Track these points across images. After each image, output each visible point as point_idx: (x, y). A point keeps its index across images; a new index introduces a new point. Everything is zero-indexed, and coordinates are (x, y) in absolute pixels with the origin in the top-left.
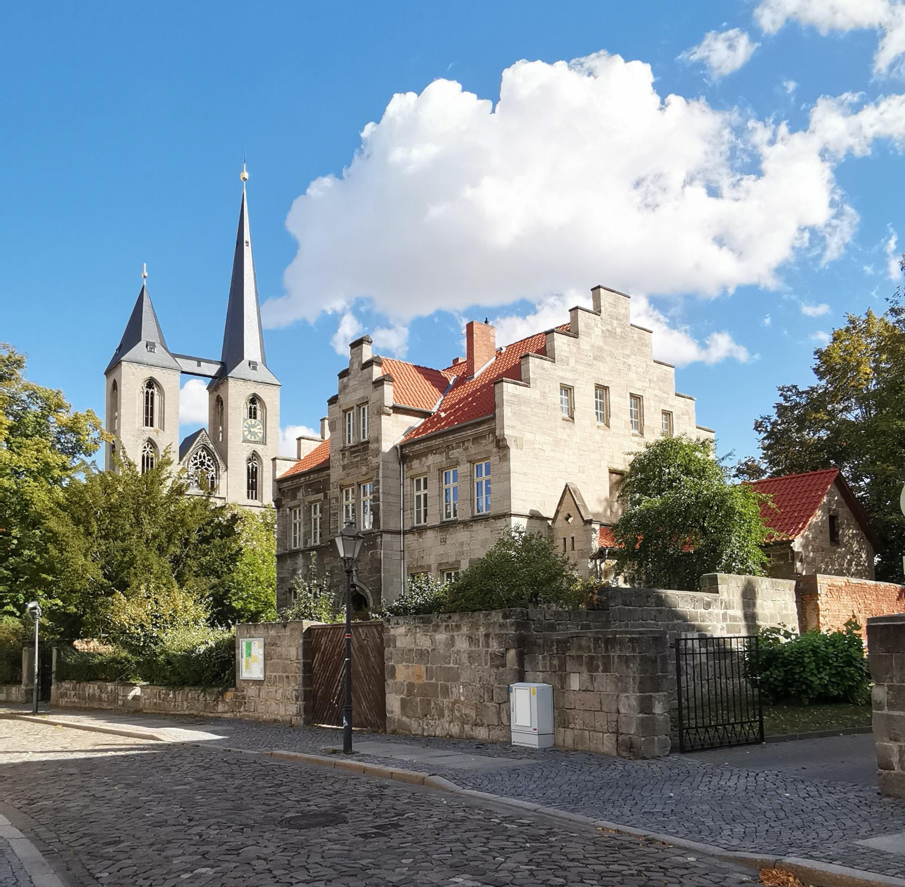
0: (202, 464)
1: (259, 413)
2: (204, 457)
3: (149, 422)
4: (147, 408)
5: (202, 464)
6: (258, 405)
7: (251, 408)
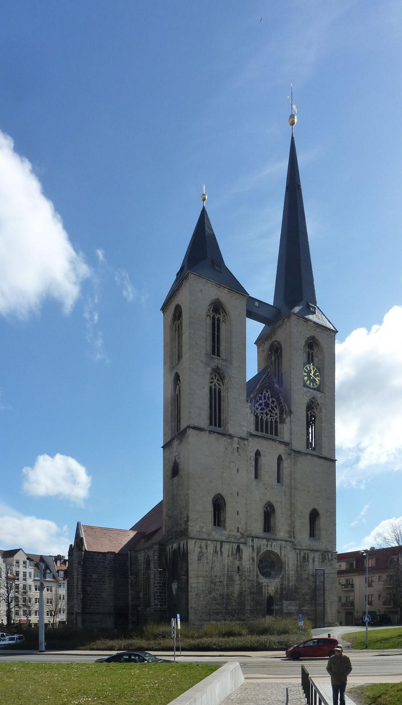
0: (267, 405)
5: (267, 405)
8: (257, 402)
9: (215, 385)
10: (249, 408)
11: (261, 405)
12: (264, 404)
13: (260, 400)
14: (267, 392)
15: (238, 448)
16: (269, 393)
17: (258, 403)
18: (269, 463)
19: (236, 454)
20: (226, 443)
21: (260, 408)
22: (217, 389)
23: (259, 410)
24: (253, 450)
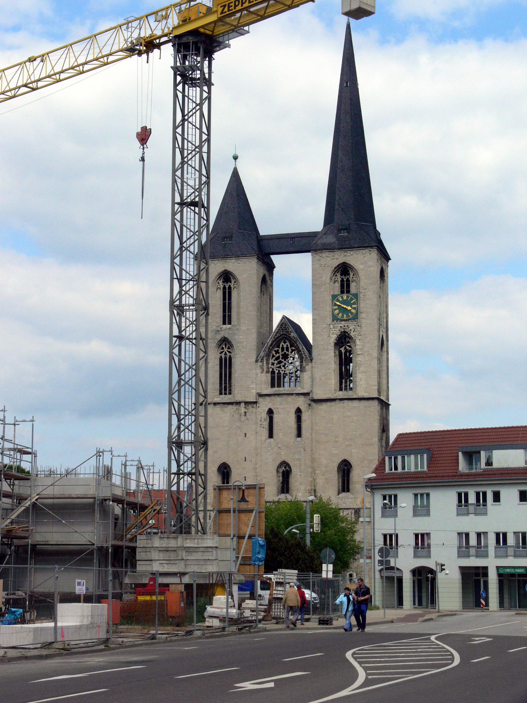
1: (353, 286)
2: (287, 349)
3: (227, 319)
4: (224, 304)
6: (351, 276)
7: (342, 281)
8: (273, 356)
9: (226, 354)
10: (259, 368)
11: (278, 358)
12: (281, 356)
13: (276, 354)
14: (285, 342)
15: (245, 412)
16: (288, 343)
17: (274, 358)
18: (285, 420)
19: (243, 418)
20: (232, 410)
21: (276, 362)
22: (228, 357)
23: (275, 365)
24: (264, 411)
